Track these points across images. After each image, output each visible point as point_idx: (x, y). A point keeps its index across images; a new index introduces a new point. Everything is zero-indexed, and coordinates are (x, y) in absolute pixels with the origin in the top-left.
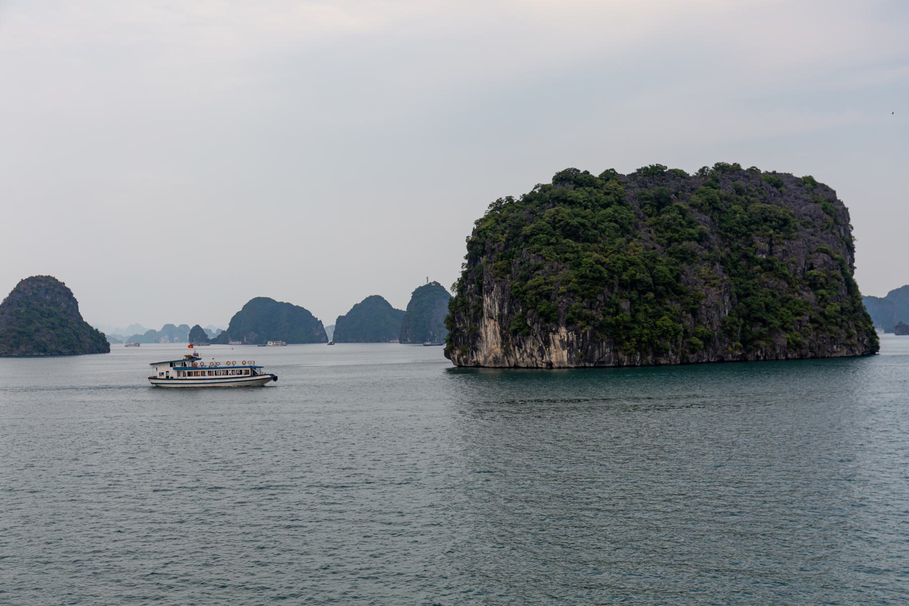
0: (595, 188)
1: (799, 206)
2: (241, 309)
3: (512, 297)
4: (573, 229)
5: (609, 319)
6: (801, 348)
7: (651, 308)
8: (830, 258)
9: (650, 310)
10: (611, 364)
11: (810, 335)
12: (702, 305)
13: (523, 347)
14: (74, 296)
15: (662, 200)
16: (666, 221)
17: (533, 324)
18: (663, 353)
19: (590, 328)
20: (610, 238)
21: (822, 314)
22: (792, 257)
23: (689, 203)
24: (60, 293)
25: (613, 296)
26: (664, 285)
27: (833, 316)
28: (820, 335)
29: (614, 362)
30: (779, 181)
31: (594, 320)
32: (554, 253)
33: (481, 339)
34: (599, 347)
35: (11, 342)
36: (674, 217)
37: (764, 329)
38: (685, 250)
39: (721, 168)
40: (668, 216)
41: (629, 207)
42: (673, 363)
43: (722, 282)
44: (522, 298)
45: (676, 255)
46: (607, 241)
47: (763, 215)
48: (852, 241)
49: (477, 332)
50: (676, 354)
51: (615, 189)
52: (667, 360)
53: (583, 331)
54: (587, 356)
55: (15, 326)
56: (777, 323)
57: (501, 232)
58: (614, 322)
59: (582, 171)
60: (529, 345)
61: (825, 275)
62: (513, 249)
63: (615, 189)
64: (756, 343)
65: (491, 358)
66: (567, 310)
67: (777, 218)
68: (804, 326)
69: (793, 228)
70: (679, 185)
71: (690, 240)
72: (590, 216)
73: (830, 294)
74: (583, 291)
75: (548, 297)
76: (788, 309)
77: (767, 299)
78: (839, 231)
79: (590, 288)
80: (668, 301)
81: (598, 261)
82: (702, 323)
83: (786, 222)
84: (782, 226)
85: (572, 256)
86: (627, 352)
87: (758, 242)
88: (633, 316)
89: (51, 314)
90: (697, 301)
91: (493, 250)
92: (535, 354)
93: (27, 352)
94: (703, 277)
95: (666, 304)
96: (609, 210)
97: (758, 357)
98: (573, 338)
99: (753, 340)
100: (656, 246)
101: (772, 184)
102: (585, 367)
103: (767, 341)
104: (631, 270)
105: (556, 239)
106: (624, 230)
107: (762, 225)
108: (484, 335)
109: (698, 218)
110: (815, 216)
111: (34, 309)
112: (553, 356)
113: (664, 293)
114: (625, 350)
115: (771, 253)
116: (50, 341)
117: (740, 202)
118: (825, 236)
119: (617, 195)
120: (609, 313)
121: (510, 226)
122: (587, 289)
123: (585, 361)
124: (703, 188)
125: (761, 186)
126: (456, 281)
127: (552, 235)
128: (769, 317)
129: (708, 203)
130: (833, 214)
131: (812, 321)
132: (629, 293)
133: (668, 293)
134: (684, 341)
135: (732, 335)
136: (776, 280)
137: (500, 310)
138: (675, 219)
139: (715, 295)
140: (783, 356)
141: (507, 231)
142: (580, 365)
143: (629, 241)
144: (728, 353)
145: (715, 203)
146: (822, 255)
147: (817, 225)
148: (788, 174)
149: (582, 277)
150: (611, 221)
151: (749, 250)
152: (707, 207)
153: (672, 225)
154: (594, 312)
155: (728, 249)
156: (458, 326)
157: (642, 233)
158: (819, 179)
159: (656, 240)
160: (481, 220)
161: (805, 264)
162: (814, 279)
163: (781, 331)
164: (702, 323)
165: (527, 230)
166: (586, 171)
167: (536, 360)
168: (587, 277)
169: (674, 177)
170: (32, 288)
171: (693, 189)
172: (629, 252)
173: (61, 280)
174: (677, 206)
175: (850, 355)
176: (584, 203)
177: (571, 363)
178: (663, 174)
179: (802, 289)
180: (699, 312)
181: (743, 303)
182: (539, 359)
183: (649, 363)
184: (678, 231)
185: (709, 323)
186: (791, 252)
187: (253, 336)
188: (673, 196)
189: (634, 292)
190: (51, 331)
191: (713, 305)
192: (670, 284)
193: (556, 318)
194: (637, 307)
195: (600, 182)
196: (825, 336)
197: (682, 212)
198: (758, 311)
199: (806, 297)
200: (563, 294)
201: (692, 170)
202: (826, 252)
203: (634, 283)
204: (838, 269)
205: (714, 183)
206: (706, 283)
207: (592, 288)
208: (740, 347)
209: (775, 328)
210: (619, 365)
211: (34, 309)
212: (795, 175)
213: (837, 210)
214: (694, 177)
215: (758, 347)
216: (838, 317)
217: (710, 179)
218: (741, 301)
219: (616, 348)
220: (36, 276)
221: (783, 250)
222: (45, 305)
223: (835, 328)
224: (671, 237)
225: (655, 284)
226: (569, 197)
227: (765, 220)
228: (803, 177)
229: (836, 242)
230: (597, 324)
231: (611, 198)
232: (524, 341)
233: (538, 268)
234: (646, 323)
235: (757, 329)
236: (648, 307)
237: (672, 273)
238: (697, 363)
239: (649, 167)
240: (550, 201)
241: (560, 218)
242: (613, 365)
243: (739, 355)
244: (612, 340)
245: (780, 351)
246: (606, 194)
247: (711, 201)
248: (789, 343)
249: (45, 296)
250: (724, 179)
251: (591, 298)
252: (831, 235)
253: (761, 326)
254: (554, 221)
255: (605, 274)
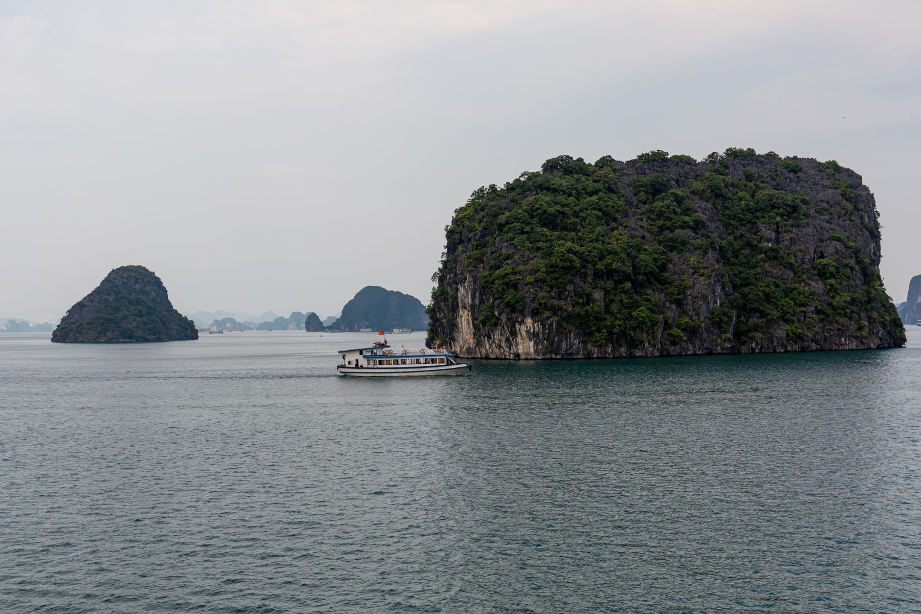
0: (584, 174)
1: (816, 193)
2: (353, 298)
3: (483, 288)
4: (550, 217)
5: (578, 309)
6: (803, 341)
7: (627, 299)
8: (843, 246)
9: (626, 301)
10: (580, 356)
11: (815, 327)
12: (688, 295)
13: (492, 337)
14: (164, 285)
15: (657, 187)
16: (658, 209)
17: (500, 314)
18: (638, 345)
19: (556, 318)
20: (591, 227)
21: (830, 305)
22: (800, 245)
23: (689, 190)
24: (149, 282)
25: (586, 286)
26: (645, 274)
27: (841, 307)
28: (827, 327)
29: (582, 354)
30: (797, 167)
31: (561, 310)
32: (527, 244)
33: (458, 329)
34: (566, 338)
35: (99, 329)
36: (667, 205)
37: (760, 320)
38: (675, 239)
39: (733, 154)
40: (661, 204)
41: (620, 195)
42: (650, 355)
43: (712, 271)
44: (491, 288)
45: (666, 243)
46: (587, 229)
47: (770, 202)
48: (877, 229)
49: (454, 322)
50: (654, 346)
51: (606, 176)
52: (642, 352)
53: (549, 322)
54: (553, 348)
55: (104, 313)
56: (776, 314)
57: (478, 221)
58: (582, 313)
59: (575, 159)
60: (497, 336)
61: (835, 264)
62: (488, 238)
63: (606, 176)
64: (751, 334)
65: (465, 348)
66: (533, 301)
67: (785, 205)
68: (809, 318)
69: (804, 215)
70: (682, 172)
71: (683, 227)
72: (574, 204)
73: (840, 284)
74: (551, 281)
75: (515, 287)
76: (792, 300)
77: (767, 289)
78: (861, 217)
79: (559, 278)
80: (649, 291)
81: (571, 249)
82: (688, 315)
83: (795, 209)
84: (792, 213)
85: (545, 244)
86: (596, 344)
87: (764, 229)
88: (607, 307)
89: (138, 302)
90: (682, 290)
91: (470, 239)
92: (503, 344)
93: (113, 338)
94: (692, 266)
95: (646, 294)
96: (594, 198)
97: (752, 348)
98: (539, 329)
99: (749, 331)
100: (646, 234)
101: (789, 170)
102: (552, 359)
103: (763, 333)
104: (608, 260)
105: (532, 228)
106: (608, 217)
107: (768, 212)
108: (460, 325)
109: (698, 205)
110: (833, 202)
111: (122, 298)
112: (520, 346)
113: (646, 284)
114: (595, 342)
115: (778, 241)
116: (136, 328)
117: (748, 188)
118: (842, 223)
119: (607, 183)
120: (578, 304)
121: (487, 213)
122: (556, 279)
123: (551, 352)
124: (707, 174)
125: (776, 171)
126: (436, 270)
127: (528, 224)
128: (767, 308)
129: (709, 190)
130: (853, 200)
131: (818, 312)
132: (605, 283)
133: (650, 283)
134: (665, 333)
135: (722, 326)
136: (780, 270)
137: (473, 298)
138: (668, 207)
139: (703, 285)
140: (782, 348)
141: (485, 220)
142: (547, 357)
143: (613, 229)
144: (716, 346)
145: (718, 189)
146: (834, 243)
147: (834, 212)
148: (812, 159)
149: (552, 266)
150: (595, 209)
151: (753, 238)
152: (708, 193)
153: (665, 212)
154: (562, 303)
155: (731, 238)
156: (438, 316)
157: (632, 222)
158: (842, 164)
159: (646, 227)
160: (461, 208)
161: (815, 252)
162: (824, 268)
163: (780, 322)
164: (688, 315)
165: (502, 219)
166: (580, 158)
167: (504, 351)
168: (557, 266)
169: (678, 164)
170: (122, 278)
171: (697, 176)
172: (611, 241)
173: (151, 270)
174: (672, 193)
175: (860, 348)
176: (567, 191)
177: (538, 354)
178: (666, 160)
179: (808, 278)
180: (684, 302)
181: (740, 294)
182: (507, 350)
183: (622, 355)
184: (671, 219)
185: (696, 314)
186: (799, 240)
187: (364, 323)
188: (673, 182)
189: (610, 281)
190: (138, 319)
191: (700, 295)
192: (652, 273)
193: (521, 308)
194: (612, 297)
195: (592, 169)
196: (832, 328)
197: (679, 200)
198: (755, 301)
199: (814, 287)
200: (531, 283)
201: (700, 156)
202: (838, 239)
203: (609, 273)
204: (851, 258)
205: (721, 169)
206: (695, 272)
207: (560, 278)
208: (729, 339)
209: (773, 320)
210: (589, 357)
211: (122, 298)
212: (819, 160)
213: (861, 196)
214: (703, 163)
215: (752, 339)
216: (847, 308)
217: (718, 165)
218: (736, 292)
219: (584, 339)
220: (127, 266)
221: (791, 238)
222: (134, 294)
223: (842, 320)
224: (663, 225)
225: (636, 274)
226: (553, 185)
227: (773, 207)
228: (826, 162)
229: (854, 230)
230: (564, 314)
231: (600, 185)
232: (492, 332)
233: (508, 258)
234: (620, 313)
235: (755, 320)
236: (624, 298)
237: (656, 262)
238: (680, 355)
239: (650, 154)
240: (533, 188)
241: (537, 206)
242: (583, 357)
243: (728, 348)
244: (581, 331)
245: (778, 343)
246: (595, 181)
247: (713, 188)
248: (788, 335)
249: (135, 285)
250: (734, 165)
251: (559, 288)
252: (848, 222)
253: (758, 317)
254: (531, 210)
255: (578, 263)
